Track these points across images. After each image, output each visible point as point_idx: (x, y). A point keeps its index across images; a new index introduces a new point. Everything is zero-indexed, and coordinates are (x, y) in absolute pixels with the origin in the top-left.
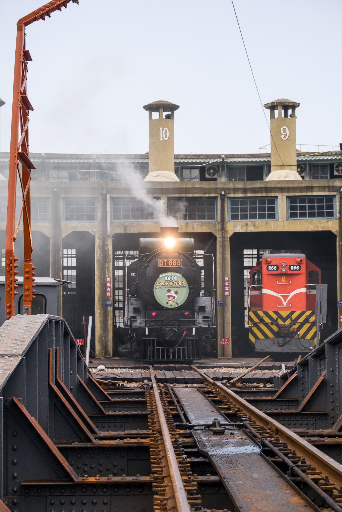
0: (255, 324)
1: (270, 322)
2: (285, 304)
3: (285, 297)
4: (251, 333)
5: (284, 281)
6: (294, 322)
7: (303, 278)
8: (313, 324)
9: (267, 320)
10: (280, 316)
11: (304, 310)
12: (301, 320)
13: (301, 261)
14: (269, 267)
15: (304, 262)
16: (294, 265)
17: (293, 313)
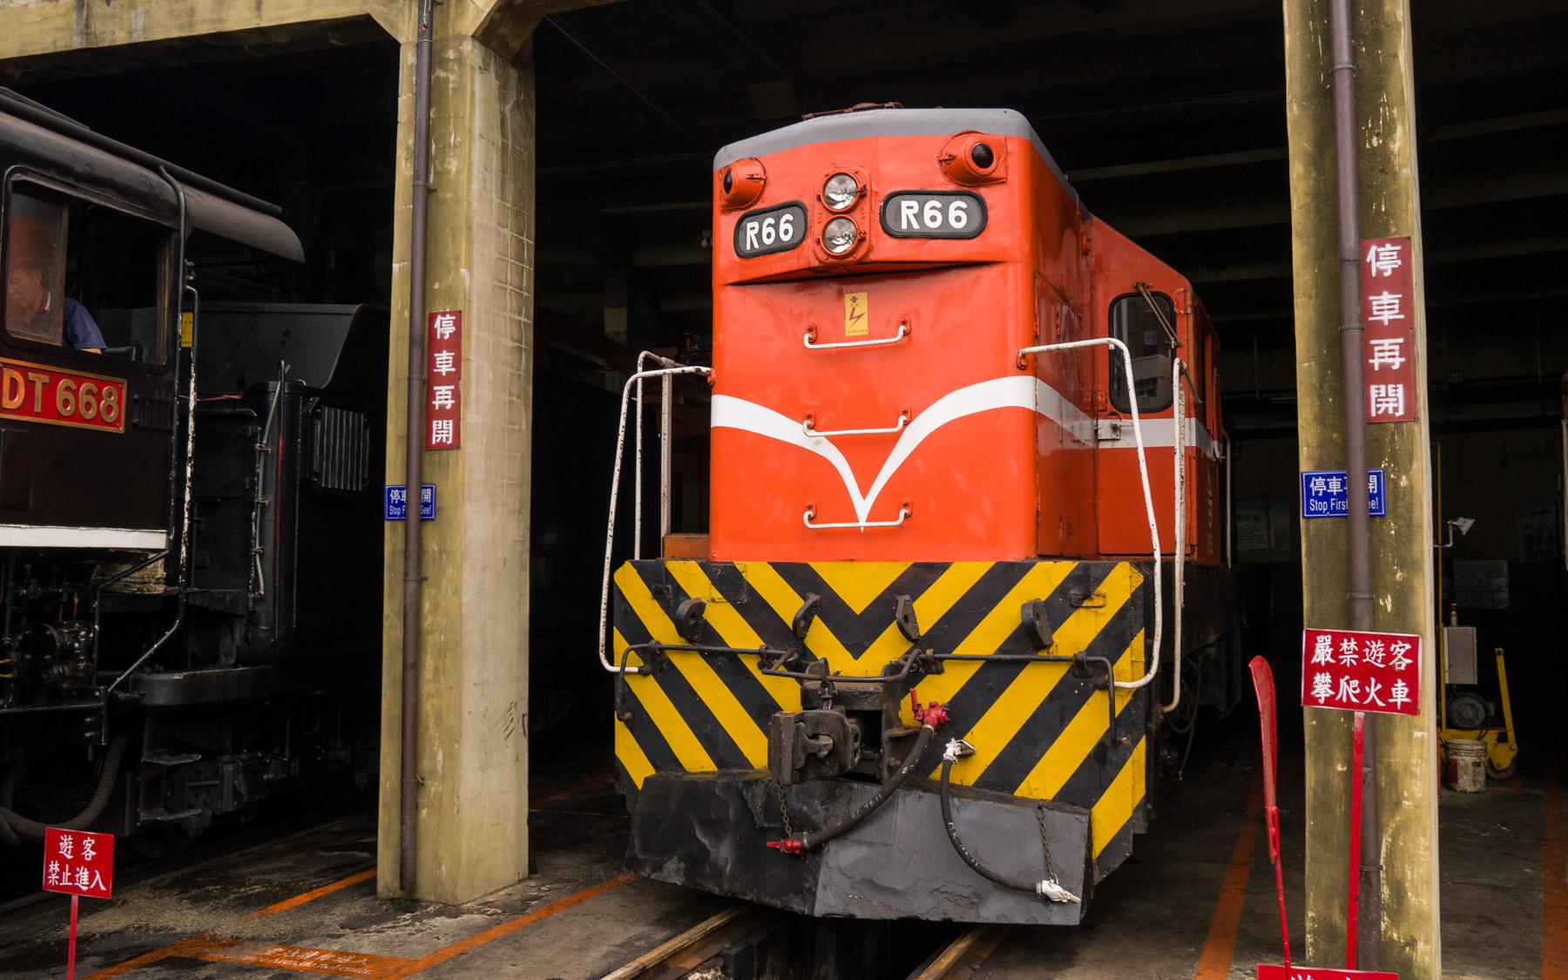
0: (657, 663)
1: (754, 642)
2: (863, 507)
3: (867, 454)
4: (632, 726)
5: (861, 326)
6: (931, 651)
7: (1002, 294)
8: (1087, 674)
9: (737, 633)
10: (827, 606)
11: (1015, 556)
12: (987, 638)
13: (984, 157)
14: (752, 228)
15: (1014, 167)
16: (922, 194)
17: (922, 576)
